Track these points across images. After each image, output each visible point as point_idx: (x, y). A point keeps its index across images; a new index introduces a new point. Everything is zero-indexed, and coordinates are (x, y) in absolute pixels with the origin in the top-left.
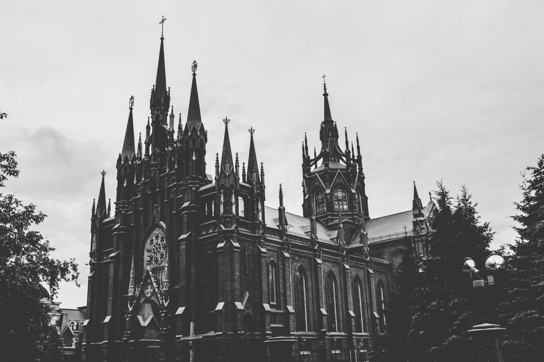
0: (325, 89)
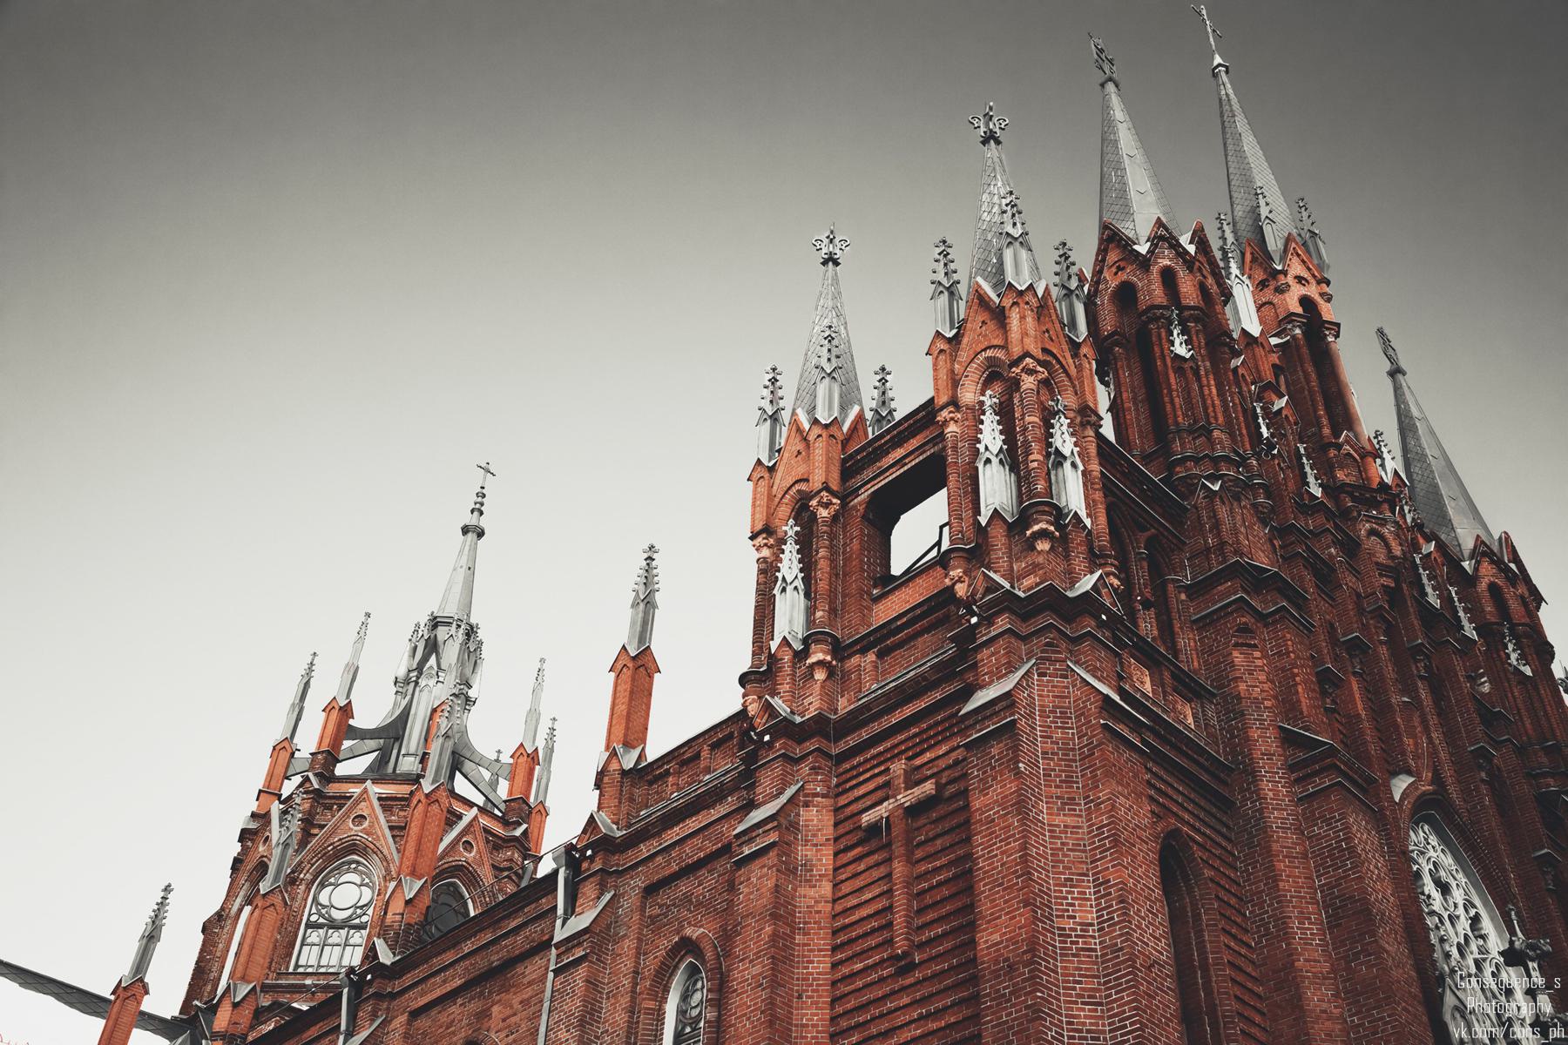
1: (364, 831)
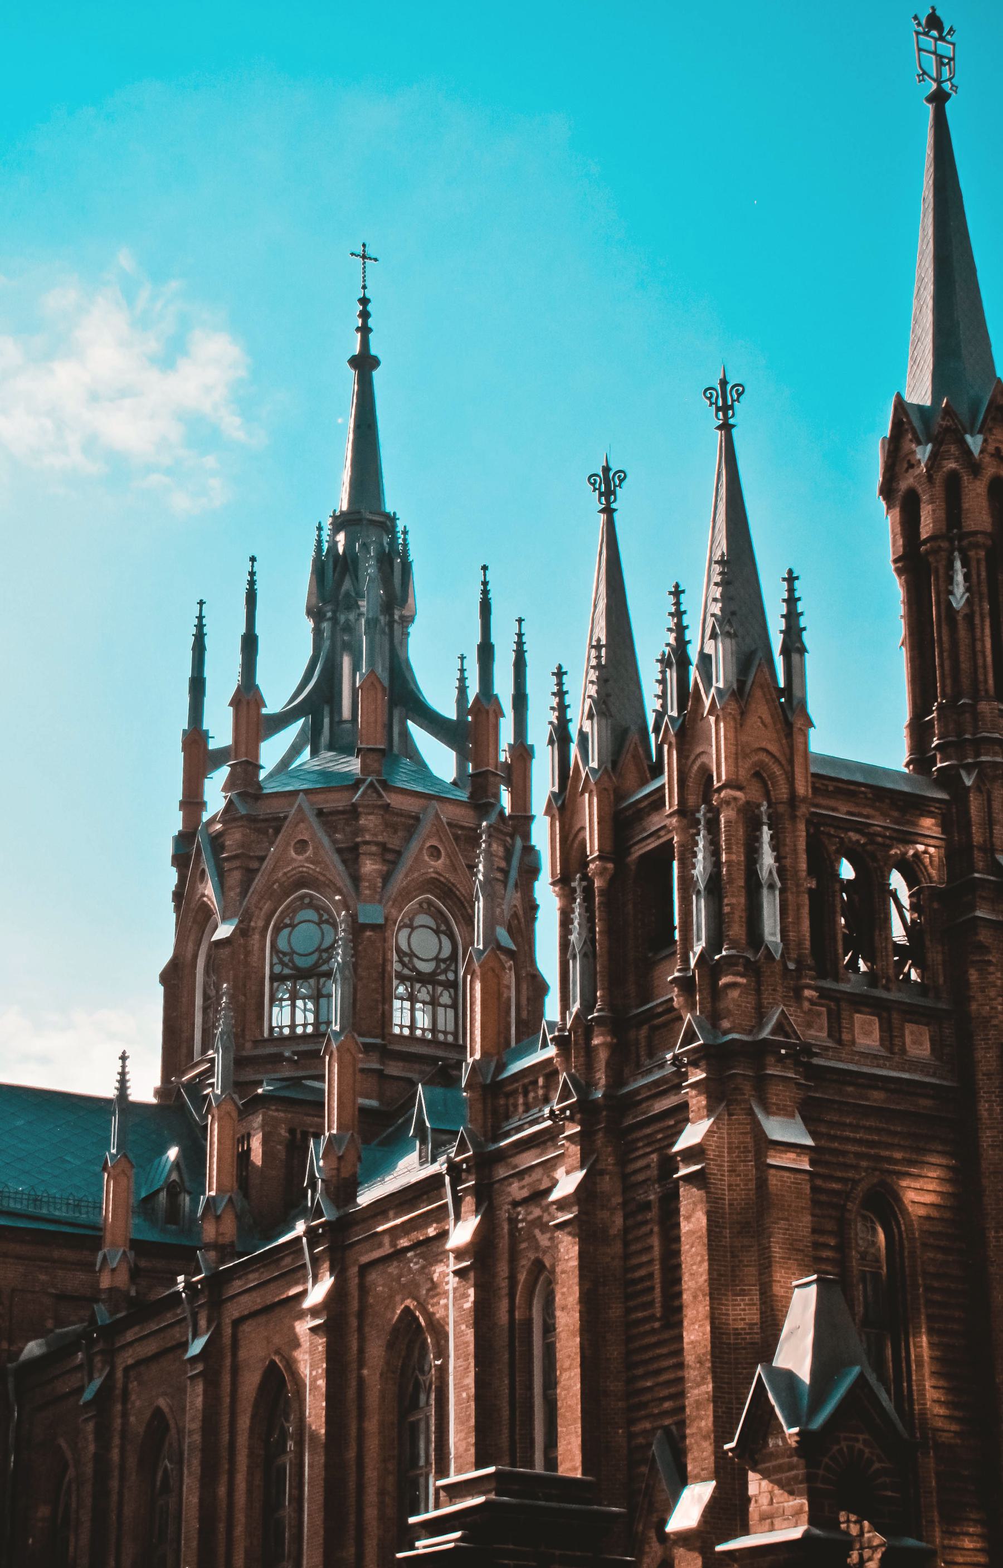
0: (365, 330)
1: (308, 860)
